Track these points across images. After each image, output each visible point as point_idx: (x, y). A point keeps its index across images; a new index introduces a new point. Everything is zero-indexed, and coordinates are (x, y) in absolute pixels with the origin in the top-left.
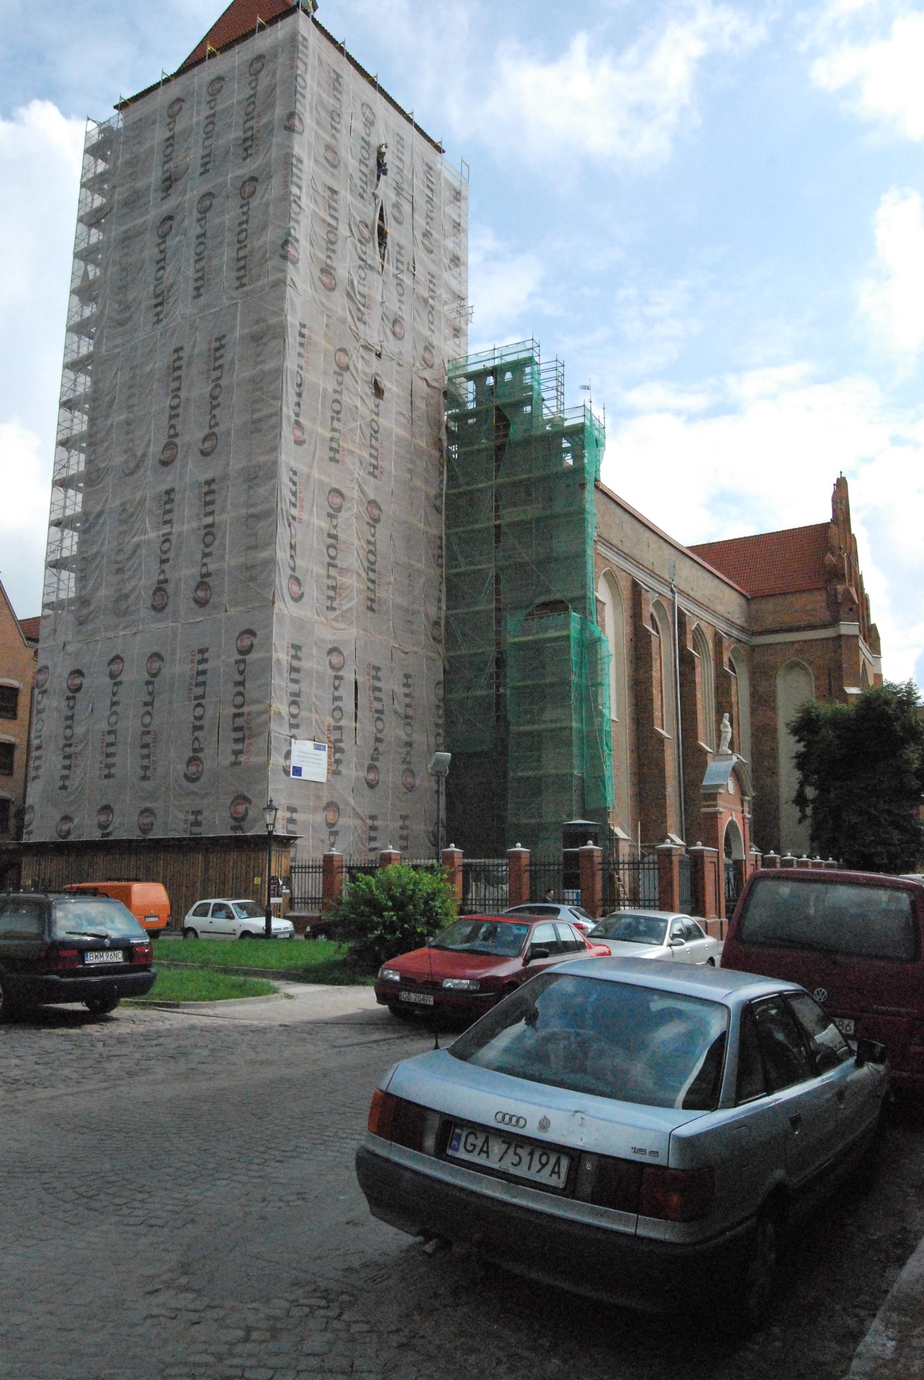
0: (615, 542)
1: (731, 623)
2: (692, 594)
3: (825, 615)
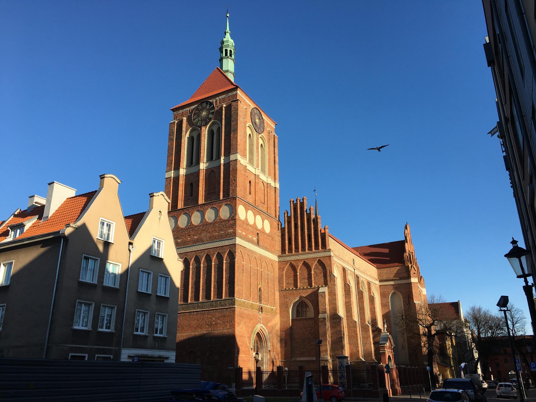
0: (338, 255)
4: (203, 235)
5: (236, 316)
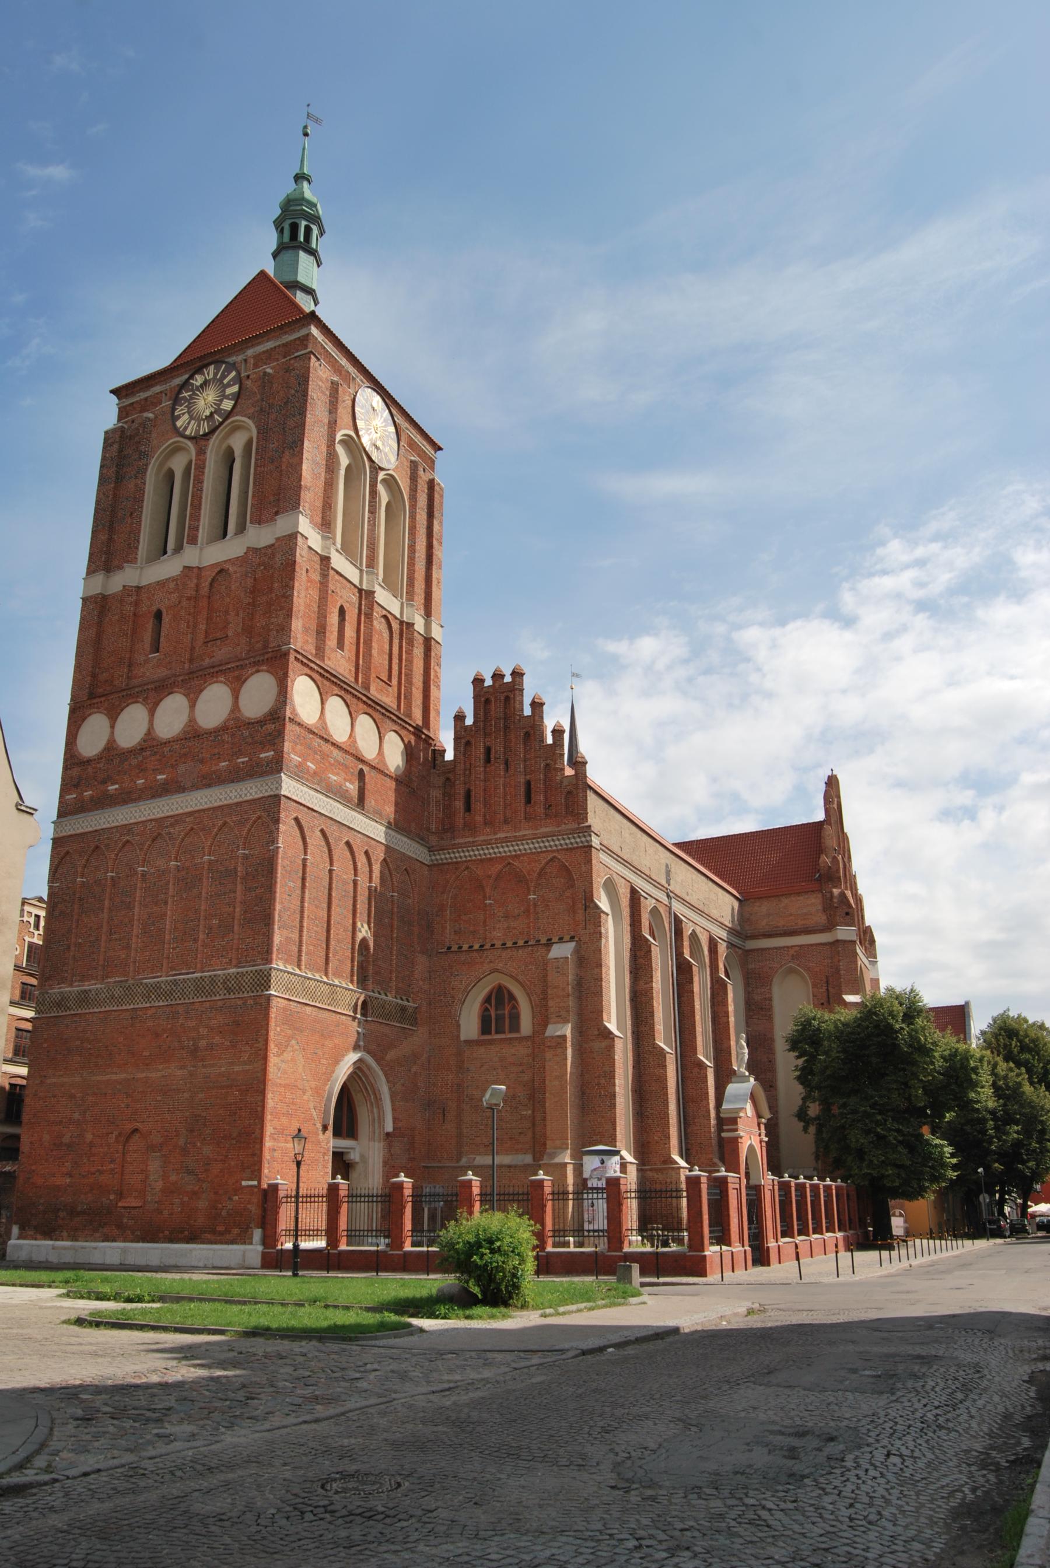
1: (722, 925)
2: (687, 898)
3: (822, 919)
4: (181, 769)
5: (272, 1024)
